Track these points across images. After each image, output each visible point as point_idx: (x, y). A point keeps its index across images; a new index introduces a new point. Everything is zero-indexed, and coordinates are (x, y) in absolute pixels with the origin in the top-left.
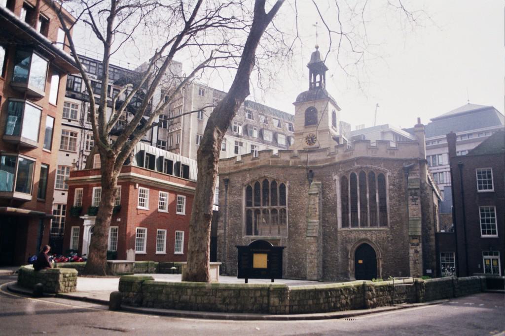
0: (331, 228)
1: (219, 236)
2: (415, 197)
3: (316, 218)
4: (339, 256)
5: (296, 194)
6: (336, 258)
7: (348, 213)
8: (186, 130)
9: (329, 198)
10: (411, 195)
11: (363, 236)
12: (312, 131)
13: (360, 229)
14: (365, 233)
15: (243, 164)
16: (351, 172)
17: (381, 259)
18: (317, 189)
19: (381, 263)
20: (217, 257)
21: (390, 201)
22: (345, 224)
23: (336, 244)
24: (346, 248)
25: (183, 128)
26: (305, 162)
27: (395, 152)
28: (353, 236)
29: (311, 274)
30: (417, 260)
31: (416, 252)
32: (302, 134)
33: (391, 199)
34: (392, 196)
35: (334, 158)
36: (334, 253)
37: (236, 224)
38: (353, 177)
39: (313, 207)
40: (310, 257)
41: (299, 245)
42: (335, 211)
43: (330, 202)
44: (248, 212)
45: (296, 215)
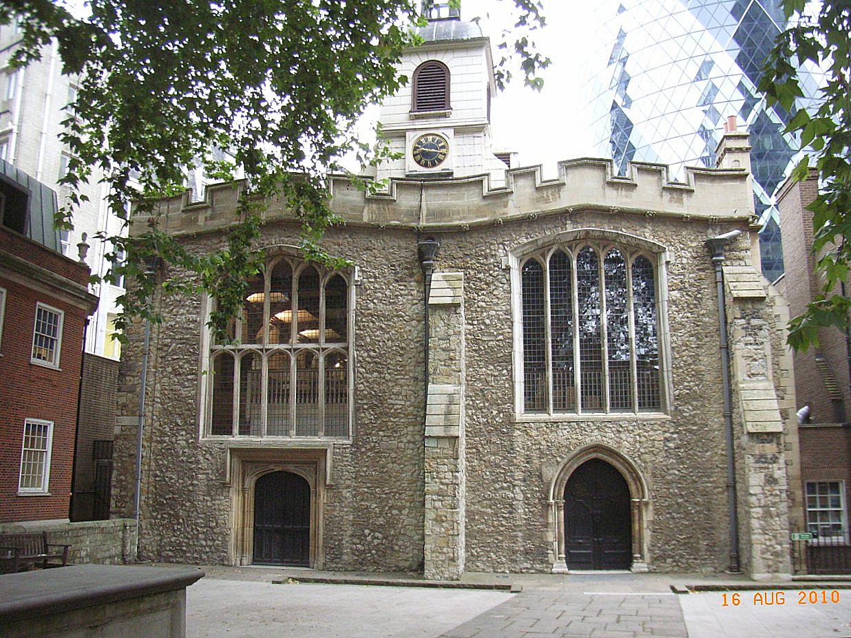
0: (495, 412)
1: (117, 437)
2: (754, 322)
3: (451, 379)
4: (520, 497)
5: (381, 306)
6: (511, 505)
7: (544, 370)
8: (28, 132)
9: (488, 322)
10: (743, 318)
11: (594, 438)
13: (581, 415)
14: (598, 428)
15: (209, 212)
16: (554, 248)
17: (647, 504)
19: (648, 516)
20: (113, 502)
21: (672, 336)
22: (535, 402)
23: (511, 463)
24: (540, 476)
25: (19, 127)
27: (684, 196)
28: (563, 434)
29: (442, 557)
30: (774, 504)
31: (771, 480)
32: (401, 135)
33: (674, 329)
34: (678, 319)
35: (506, 206)
36: (502, 488)
37: (179, 399)
38: (561, 261)
39: (444, 345)
40: (438, 504)
41: (390, 465)
42: (509, 360)
43: (491, 334)
44: (223, 363)
45: (380, 373)
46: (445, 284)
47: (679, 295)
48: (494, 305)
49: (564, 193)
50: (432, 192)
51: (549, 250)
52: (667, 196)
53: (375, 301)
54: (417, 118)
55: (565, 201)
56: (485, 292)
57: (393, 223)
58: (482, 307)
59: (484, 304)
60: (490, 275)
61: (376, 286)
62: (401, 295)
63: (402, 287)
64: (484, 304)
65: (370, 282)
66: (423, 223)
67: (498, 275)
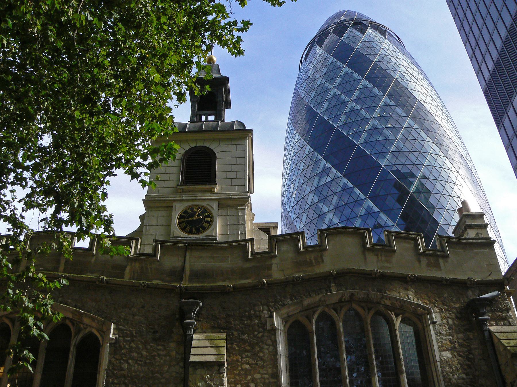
12: (197, 197)
16: (320, 310)
18: (213, 351)
26: (178, 274)
27: (441, 261)
35: (269, 268)
46: (207, 343)
47: (450, 356)
48: (259, 367)
49: (327, 257)
50: (196, 254)
51: (314, 313)
52: (424, 261)
53: (130, 361)
54: (183, 191)
55: (328, 265)
56: (249, 354)
57: (155, 282)
58: (246, 369)
59: (248, 367)
60: (255, 336)
61: (133, 345)
62: (159, 355)
63: (160, 347)
64: (248, 367)
65: (126, 341)
66: (184, 285)
67: (262, 336)
